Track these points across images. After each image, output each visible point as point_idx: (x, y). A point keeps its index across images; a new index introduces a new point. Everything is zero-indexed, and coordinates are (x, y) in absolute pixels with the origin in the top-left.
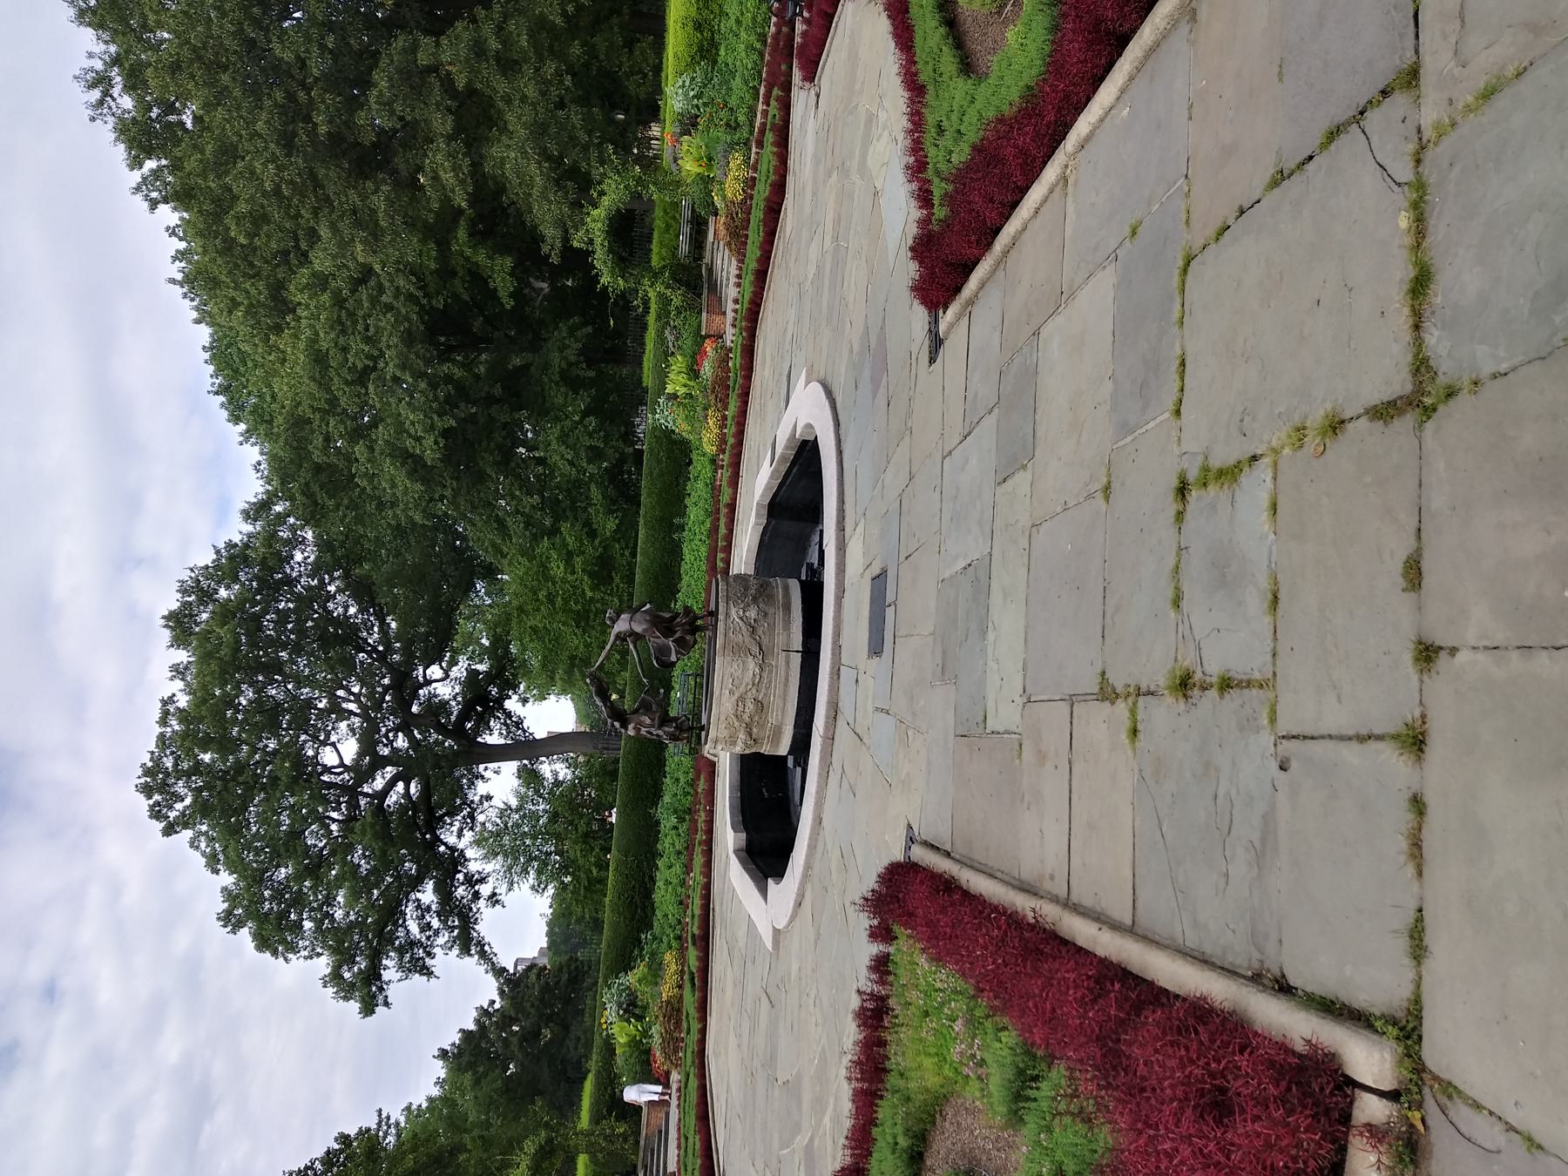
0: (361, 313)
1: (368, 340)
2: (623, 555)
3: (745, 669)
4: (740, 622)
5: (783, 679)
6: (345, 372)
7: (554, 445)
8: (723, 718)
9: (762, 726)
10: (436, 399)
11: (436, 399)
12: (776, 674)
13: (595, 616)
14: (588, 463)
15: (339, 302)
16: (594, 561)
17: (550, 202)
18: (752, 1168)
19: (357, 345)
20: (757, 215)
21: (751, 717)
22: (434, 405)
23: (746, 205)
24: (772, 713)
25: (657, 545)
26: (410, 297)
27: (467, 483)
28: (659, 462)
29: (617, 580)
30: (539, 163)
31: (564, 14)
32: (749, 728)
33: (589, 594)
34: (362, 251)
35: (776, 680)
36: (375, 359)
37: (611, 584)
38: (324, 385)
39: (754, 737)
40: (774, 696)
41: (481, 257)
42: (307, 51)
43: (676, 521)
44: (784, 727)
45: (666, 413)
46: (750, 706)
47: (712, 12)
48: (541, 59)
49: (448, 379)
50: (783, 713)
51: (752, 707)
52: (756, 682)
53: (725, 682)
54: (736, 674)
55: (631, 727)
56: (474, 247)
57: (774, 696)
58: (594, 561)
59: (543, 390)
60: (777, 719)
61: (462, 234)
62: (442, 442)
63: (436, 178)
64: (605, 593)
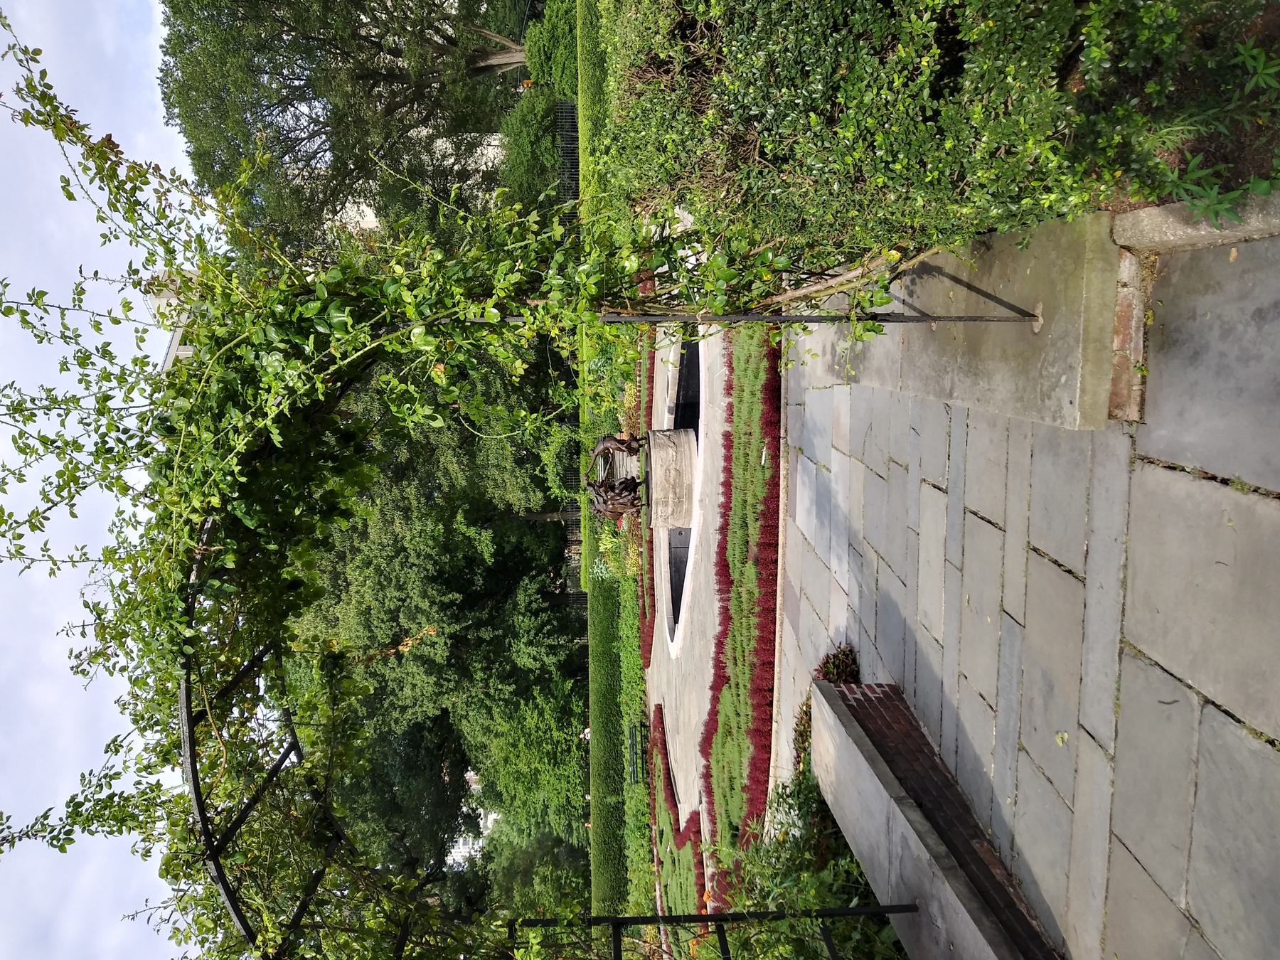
1: (400, 588)
3: (667, 454)
6: (382, 616)
9: (681, 486)
15: (379, 571)
17: (517, 477)
18: (719, 830)
19: (392, 592)
20: (642, 412)
23: (638, 407)
25: (603, 672)
32: (674, 487)
36: (404, 600)
38: (368, 626)
41: (472, 532)
46: (673, 473)
48: (508, 396)
49: (452, 603)
56: (468, 526)
61: (460, 517)
62: (449, 642)
63: (446, 472)
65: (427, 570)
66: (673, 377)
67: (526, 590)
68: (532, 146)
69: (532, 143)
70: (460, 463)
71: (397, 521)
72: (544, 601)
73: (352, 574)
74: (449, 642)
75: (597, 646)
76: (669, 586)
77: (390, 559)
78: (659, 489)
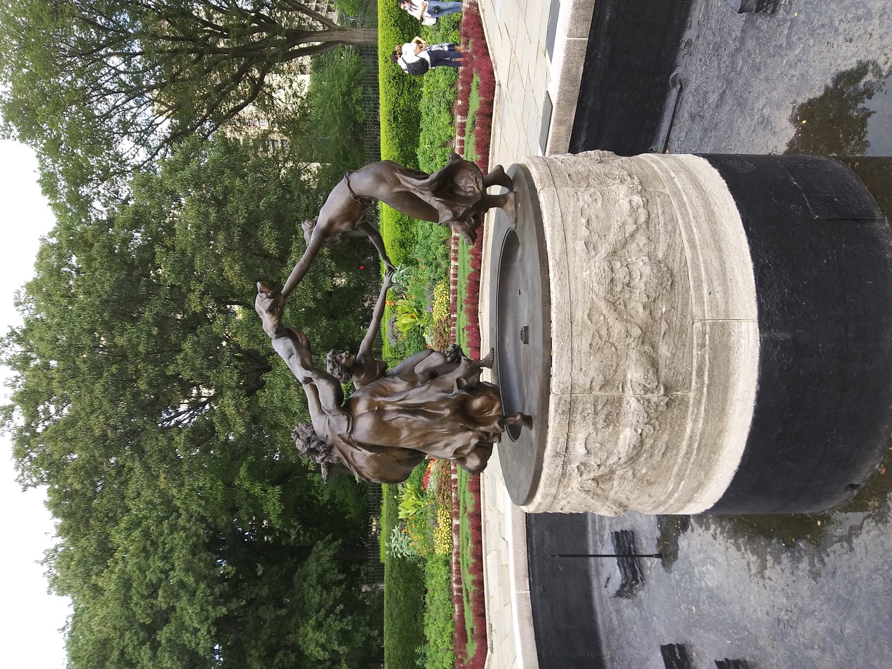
0: (162, 539)
1: (165, 558)
3: (607, 201)
5: (701, 211)
7: (311, 635)
8: (580, 315)
9: (680, 334)
10: (212, 594)
11: (212, 594)
12: (682, 204)
14: (340, 644)
15: (146, 534)
21: (650, 306)
22: (210, 598)
24: (698, 288)
26: (203, 519)
28: (397, 601)
31: (315, 299)
32: (647, 337)
34: (165, 478)
35: (685, 215)
39: (663, 372)
40: (693, 246)
41: (257, 490)
42: (138, 337)
43: (418, 650)
44: (735, 328)
45: (400, 539)
47: (411, 233)
50: (724, 284)
51: (647, 270)
52: (642, 218)
53: (570, 227)
54: (591, 212)
57: (693, 246)
59: (303, 596)
60: (714, 306)
61: (243, 472)
65: (198, 536)
66: (563, 92)
67: (318, 559)
68: (343, 97)
69: (343, 95)
70: (237, 407)
71: (163, 476)
72: (340, 572)
73: (117, 538)
74: (214, 630)
75: (395, 648)
76: (530, 631)
77: (160, 521)
78: (582, 344)
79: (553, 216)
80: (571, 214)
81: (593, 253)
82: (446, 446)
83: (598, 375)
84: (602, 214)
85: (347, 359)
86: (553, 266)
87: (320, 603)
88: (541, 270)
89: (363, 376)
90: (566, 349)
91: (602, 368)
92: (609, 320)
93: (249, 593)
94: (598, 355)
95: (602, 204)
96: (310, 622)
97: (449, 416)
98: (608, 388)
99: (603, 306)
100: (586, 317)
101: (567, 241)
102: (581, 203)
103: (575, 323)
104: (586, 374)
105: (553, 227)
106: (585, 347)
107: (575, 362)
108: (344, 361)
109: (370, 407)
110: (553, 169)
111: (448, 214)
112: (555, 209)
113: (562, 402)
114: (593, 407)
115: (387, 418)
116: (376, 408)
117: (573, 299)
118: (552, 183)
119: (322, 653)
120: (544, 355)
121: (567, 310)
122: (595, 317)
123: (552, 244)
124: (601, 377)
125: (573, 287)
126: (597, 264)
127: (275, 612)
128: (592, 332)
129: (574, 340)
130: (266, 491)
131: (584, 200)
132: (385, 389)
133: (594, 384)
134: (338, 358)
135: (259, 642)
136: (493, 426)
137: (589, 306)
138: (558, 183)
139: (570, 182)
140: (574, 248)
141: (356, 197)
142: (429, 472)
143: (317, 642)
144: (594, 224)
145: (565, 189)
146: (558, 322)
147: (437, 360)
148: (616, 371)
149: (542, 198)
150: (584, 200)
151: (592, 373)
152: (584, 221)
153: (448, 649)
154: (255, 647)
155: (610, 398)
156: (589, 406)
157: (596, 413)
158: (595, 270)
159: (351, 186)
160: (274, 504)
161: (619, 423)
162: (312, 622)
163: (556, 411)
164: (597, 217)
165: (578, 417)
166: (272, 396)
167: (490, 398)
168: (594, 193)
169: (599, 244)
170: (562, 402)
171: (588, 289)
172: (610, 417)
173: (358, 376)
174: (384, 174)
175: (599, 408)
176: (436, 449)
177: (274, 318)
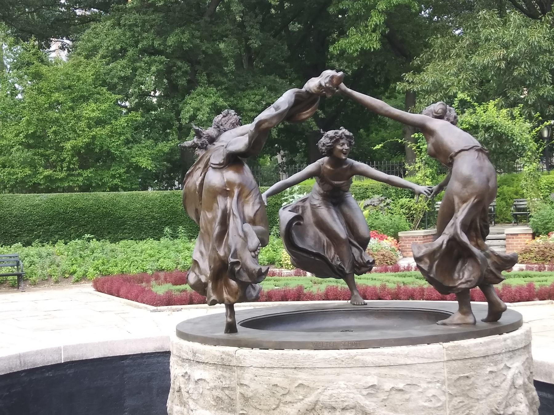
2: (113, 177)
4: (506, 385)
7: (207, 101)
8: (303, 377)
13: (42, 155)
16: (105, 148)
17: (457, 75)
25: (145, 211)
27: (154, 20)
29: (87, 173)
30: (504, 59)
33: (68, 145)
37: (80, 168)
41: (376, 19)
53: (394, 372)
54: (414, 394)
55: (230, 175)
58: (105, 148)
59: (252, 88)
64: (70, 163)
78: (277, 378)
79: (407, 356)
80: (410, 375)
81: (365, 392)
82: (201, 253)
83: (252, 391)
84: (411, 405)
85: (341, 151)
86: (349, 354)
87: (243, 109)
88: (348, 342)
89: (329, 167)
90: (272, 362)
91: (258, 395)
92: (299, 404)
93: (251, 23)
94: (268, 392)
95: (425, 407)
96: (221, 100)
97: (218, 255)
98: (242, 400)
99: (311, 399)
100: (300, 382)
101: (378, 368)
102: (424, 385)
103: (295, 372)
104: (252, 380)
105: (393, 355)
106: (275, 380)
107: (262, 370)
108: (339, 147)
109: (230, 184)
110: (478, 361)
111: (419, 253)
112: (416, 359)
113: (230, 358)
114: (227, 386)
115: (220, 199)
116: (228, 189)
117: (317, 371)
118: (453, 358)
119: (187, 116)
120: (269, 342)
121: (307, 365)
122: (302, 391)
123: (373, 353)
124: (251, 394)
125: (329, 371)
126: (351, 395)
127: (231, 56)
128: (287, 387)
129: (281, 370)
130: (374, 31)
131: (428, 388)
132: (247, 197)
133: (245, 387)
134: (342, 141)
135: (198, 41)
136: (212, 295)
137: (311, 385)
138: (454, 364)
139: (456, 377)
140: (369, 374)
141: (452, 158)
142: (382, 238)
143: (198, 110)
144: (398, 396)
145: (446, 370)
146: (296, 356)
147: (252, 243)
148: (256, 408)
149: (435, 347)
150: (428, 388)
151: (253, 386)
152: (401, 386)
153: (178, 264)
154: (193, 36)
155: (234, 402)
156: (228, 382)
157: (223, 389)
158: (344, 393)
159: (463, 153)
160: (358, 42)
161: (216, 410)
162: (221, 102)
163: (223, 352)
164: (408, 400)
165: (220, 373)
166: (493, 26)
167: (237, 293)
168: (439, 400)
169: (375, 399)
170: (230, 358)
171: (326, 385)
172: (220, 402)
173: (329, 163)
174: (471, 186)
175: (227, 392)
176: (200, 244)
177: (315, 88)
